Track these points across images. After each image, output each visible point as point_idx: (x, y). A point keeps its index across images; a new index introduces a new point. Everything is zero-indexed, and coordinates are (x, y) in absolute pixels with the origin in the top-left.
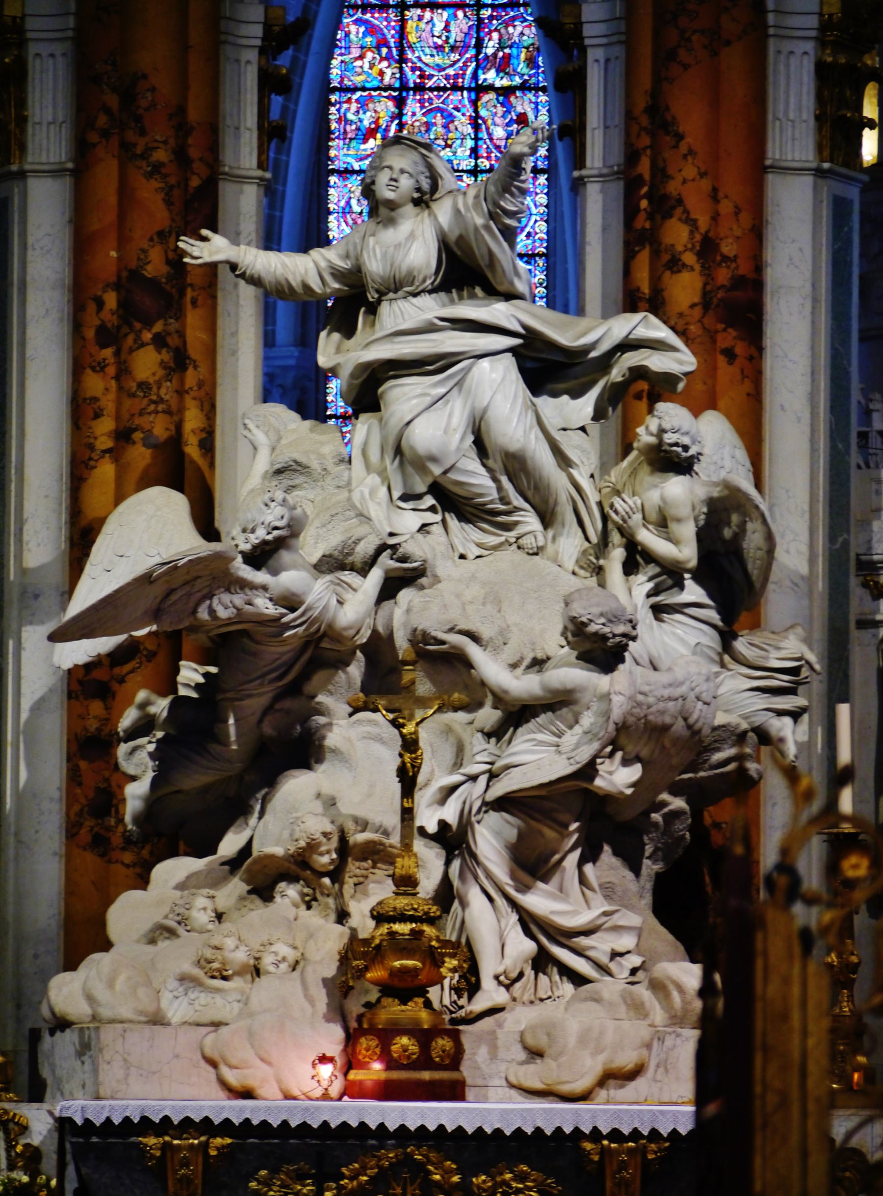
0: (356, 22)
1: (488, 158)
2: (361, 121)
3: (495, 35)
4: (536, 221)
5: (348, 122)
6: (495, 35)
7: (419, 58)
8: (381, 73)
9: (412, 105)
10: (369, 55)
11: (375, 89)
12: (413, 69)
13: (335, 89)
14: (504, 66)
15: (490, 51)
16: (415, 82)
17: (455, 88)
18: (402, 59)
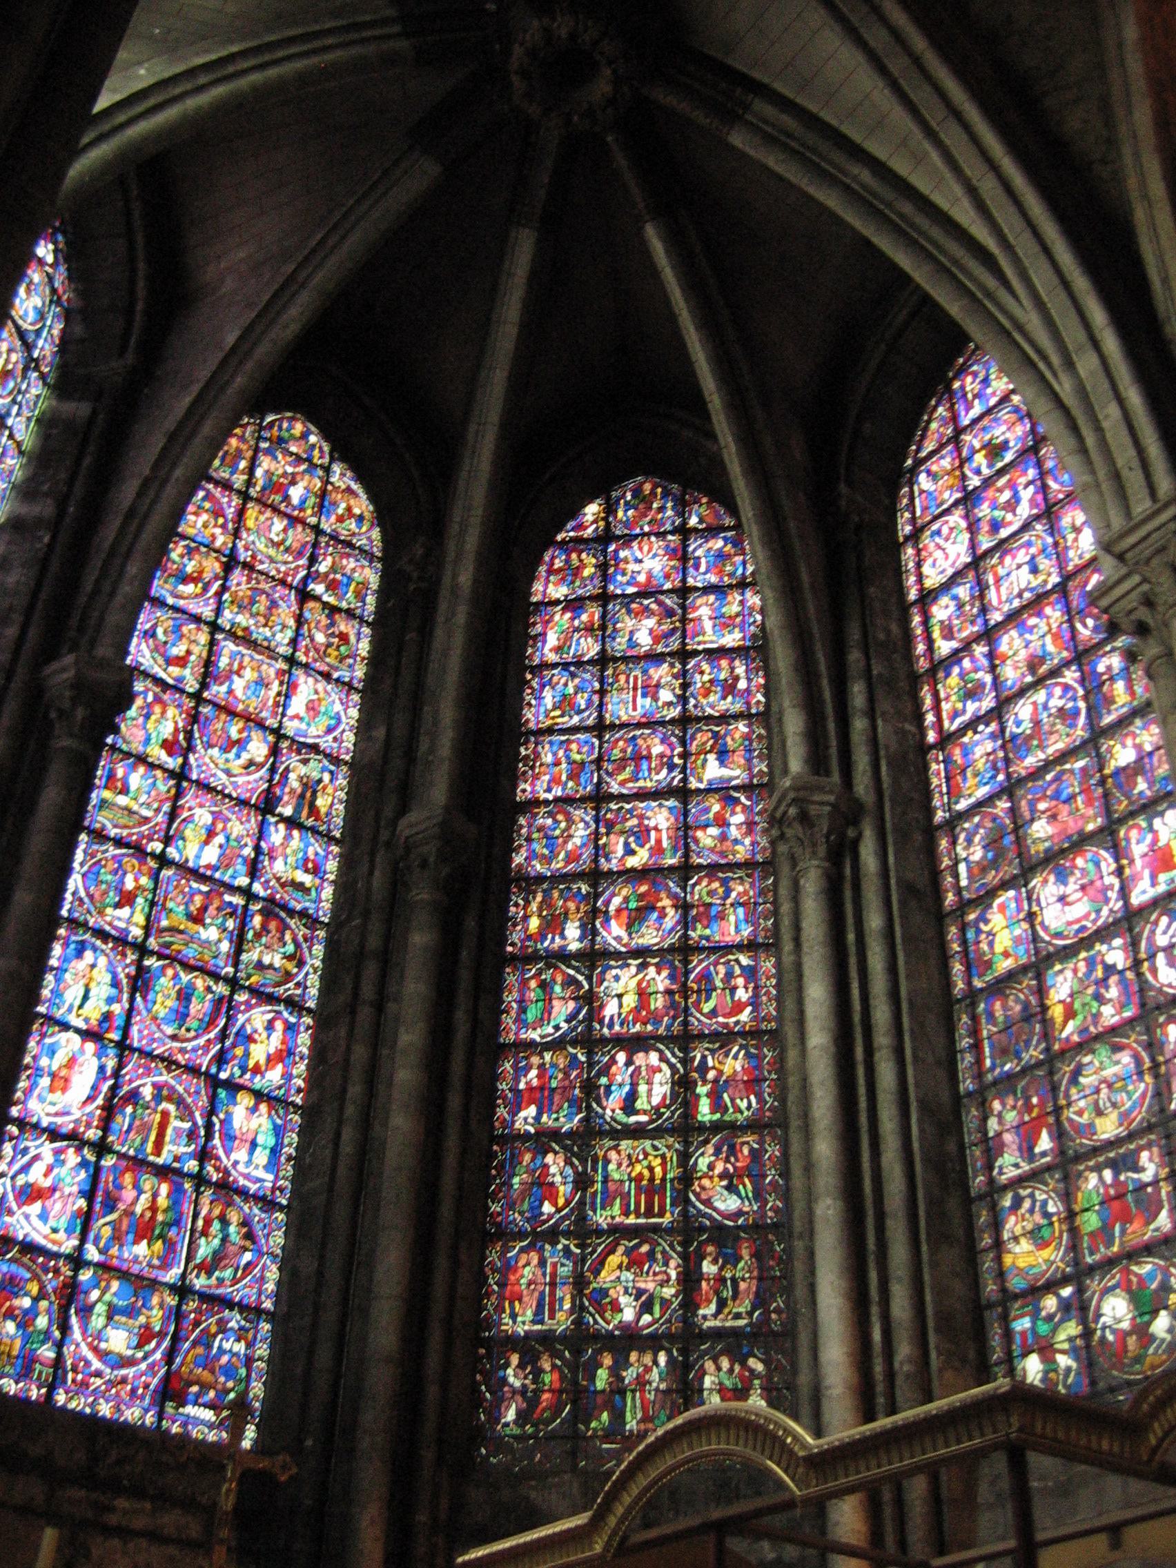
1: (306, 654)
17: (283, 582)
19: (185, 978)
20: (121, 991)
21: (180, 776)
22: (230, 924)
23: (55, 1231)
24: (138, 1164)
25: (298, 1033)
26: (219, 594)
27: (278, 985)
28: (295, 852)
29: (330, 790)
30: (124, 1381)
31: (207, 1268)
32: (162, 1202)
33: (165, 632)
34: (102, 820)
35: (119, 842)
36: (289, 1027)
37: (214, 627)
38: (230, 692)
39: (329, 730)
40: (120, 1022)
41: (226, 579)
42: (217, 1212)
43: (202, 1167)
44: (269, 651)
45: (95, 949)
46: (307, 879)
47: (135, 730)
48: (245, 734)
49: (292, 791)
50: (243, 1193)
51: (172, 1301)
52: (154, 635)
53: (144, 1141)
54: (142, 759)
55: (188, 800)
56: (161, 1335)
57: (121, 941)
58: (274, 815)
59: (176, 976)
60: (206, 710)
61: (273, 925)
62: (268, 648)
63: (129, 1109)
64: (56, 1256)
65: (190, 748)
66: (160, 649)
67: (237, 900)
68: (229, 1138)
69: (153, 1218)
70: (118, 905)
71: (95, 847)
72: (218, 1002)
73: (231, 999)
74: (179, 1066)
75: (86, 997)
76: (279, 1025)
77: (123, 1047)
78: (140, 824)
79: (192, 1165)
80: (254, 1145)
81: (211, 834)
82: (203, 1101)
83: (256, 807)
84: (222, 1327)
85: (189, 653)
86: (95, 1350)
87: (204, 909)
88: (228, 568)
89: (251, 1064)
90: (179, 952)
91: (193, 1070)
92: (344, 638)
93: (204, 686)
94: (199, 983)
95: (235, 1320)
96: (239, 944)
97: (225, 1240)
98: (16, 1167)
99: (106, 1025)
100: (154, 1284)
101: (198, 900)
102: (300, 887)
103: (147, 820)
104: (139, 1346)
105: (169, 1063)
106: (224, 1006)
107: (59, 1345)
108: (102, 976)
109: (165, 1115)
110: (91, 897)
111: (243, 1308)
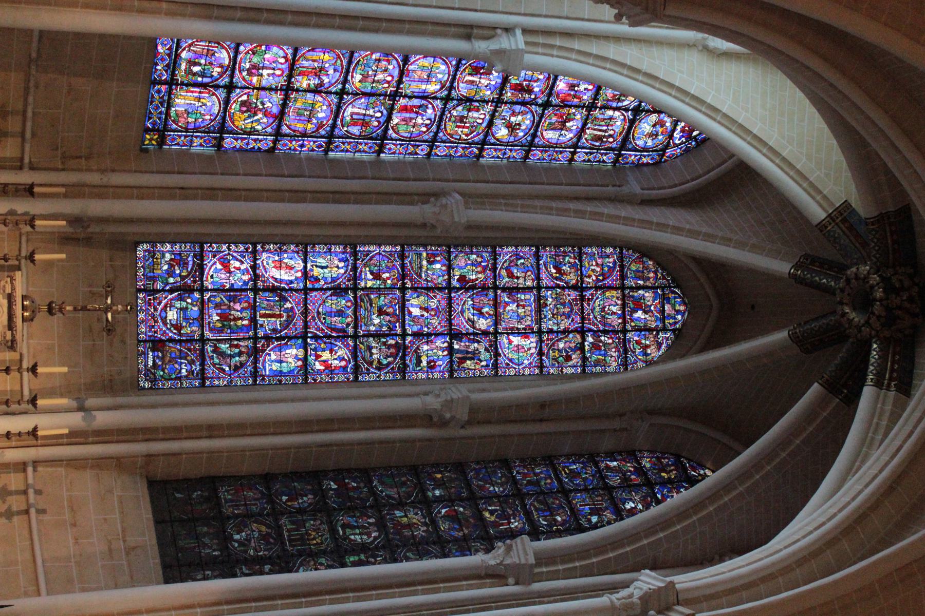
0: (614, 261)
1: (548, 339)
2: (565, 265)
3: (610, 341)
5: (564, 257)
6: (610, 341)
7: (597, 298)
8: (589, 276)
9: (574, 294)
10: (598, 269)
12: (592, 295)
13: (580, 249)
14: (595, 346)
15: (603, 338)
17: (583, 319)
18: (597, 288)
19: (350, 312)
22: (385, 329)
23: (212, 277)
24: (253, 308)
26: (558, 286)
27: (364, 359)
29: (477, 367)
30: (156, 322)
31: (216, 350)
32: (239, 323)
34: (411, 256)
35: (403, 266)
36: (345, 368)
38: (507, 304)
39: (511, 360)
40: (317, 286)
41: (569, 288)
42: (243, 350)
43: (262, 338)
44: (539, 321)
46: (424, 363)
50: (256, 361)
51: (196, 337)
52: (518, 259)
53: (265, 309)
54: (450, 268)
56: (180, 334)
57: (356, 278)
59: (349, 307)
60: (491, 294)
61: (392, 350)
62: (541, 318)
63: (277, 299)
64: (202, 281)
65: (467, 290)
66: (512, 263)
67: (399, 331)
68: (280, 348)
69: (231, 320)
70: (372, 273)
72: (343, 330)
73: (348, 337)
74: (306, 317)
75: (322, 268)
76: (343, 363)
77: (306, 291)
78: (416, 274)
79: (261, 334)
80: (281, 362)
81: (426, 309)
82: (293, 333)
83: (451, 329)
84: (192, 362)
85: (518, 278)
86: (166, 306)
87: (388, 314)
88: (574, 287)
89: (320, 353)
91: (306, 326)
92: (568, 358)
93: (504, 289)
94: (349, 319)
95: (197, 368)
96: (377, 335)
97: (231, 356)
98: (235, 254)
100: (202, 327)
101: (390, 310)
102: (419, 362)
103: (420, 277)
104: (172, 325)
105: (306, 312)
106: (342, 335)
107: (163, 290)
108: (335, 272)
109: (280, 316)
110: (371, 259)
111: (203, 370)
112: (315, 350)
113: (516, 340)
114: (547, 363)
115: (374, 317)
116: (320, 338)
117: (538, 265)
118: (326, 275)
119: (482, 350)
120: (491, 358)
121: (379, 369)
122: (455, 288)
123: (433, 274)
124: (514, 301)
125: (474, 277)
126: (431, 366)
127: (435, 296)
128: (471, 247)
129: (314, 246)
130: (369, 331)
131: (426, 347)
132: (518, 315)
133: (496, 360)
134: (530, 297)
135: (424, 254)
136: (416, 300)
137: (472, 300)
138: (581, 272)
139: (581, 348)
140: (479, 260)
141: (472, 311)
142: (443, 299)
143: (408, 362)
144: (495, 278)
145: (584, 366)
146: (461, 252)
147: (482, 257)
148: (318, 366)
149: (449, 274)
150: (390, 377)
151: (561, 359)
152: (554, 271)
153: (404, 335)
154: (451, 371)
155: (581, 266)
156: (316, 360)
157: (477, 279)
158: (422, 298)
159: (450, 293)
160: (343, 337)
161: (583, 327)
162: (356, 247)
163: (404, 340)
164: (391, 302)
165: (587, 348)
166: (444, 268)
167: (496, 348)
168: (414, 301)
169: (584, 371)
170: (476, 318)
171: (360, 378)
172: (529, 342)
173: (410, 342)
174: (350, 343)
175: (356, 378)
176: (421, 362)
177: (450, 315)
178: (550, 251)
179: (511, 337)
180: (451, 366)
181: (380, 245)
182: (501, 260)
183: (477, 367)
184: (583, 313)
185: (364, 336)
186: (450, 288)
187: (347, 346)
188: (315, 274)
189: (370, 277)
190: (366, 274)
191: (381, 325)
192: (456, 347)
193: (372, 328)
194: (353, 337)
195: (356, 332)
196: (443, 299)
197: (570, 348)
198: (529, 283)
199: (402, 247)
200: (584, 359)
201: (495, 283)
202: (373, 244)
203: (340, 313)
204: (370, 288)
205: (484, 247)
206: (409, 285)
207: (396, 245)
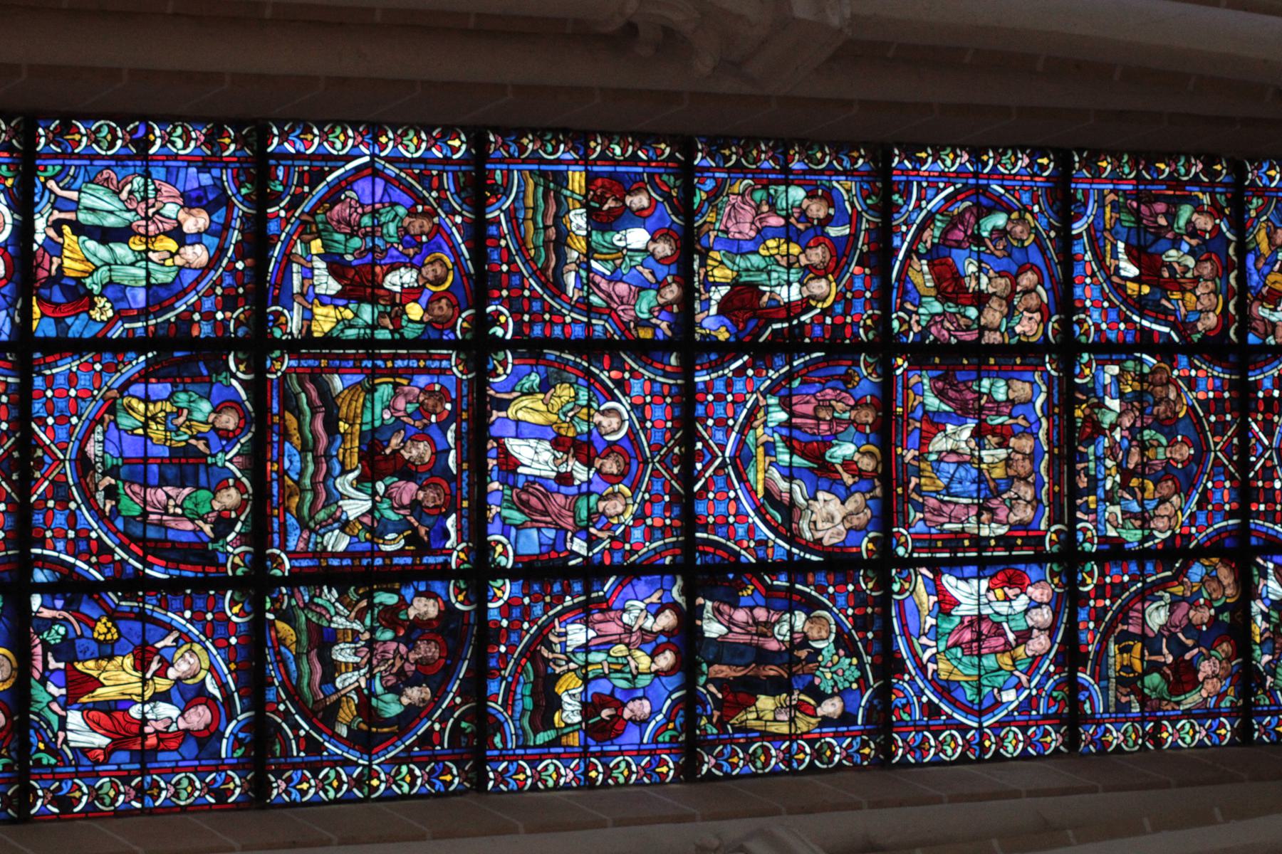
1: (1100, 590)
2: (1175, 244)
4: (963, 729)
5: (1174, 204)
11: (1242, 279)
13: (1238, 170)
16: (1258, 385)
17: (1245, 493)
19: (229, 460)
20: (144, 313)
21: (686, 345)
22: (393, 543)
25: (201, 772)
26: (1147, 341)
27: (294, 693)
28: (621, 667)
29: (803, 724)
33: (1000, 233)
34: (519, 188)
35: (478, 232)
36: (207, 739)
37: (1066, 348)
38: (934, 423)
39: (945, 689)
40: (77, 327)
41: (1189, 349)
45: (221, 232)
46: (571, 712)
47: (747, 214)
48: (848, 479)
49: (766, 629)
52: (983, 211)
54: (688, 246)
55: (642, 380)
58: (688, 592)
59: (228, 437)
60: (866, 376)
61: (427, 650)
62: (1075, 492)
65: (762, 355)
66: (960, 229)
67: (456, 550)
70: (337, 267)
71: (448, 182)
72: (198, 552)
73: (223, 583)
74: (25, 486)
75: (105, 235)
76: (199, 717)
78: (539, 274)
81: (583, 448)
83: (690, 545)
85: (981, 300)
87: (407, 471)
88: (1212, 348)
89: (89, 667)
90: (285, 435)
92: (1183, 677)
93: (921, 354)
94: (230, 498)
96: (357, 576)
99: (58, 296)
101: (420, 451)
102: (547, 703)
103: (558, 288)
106: (195, 574)
110: (333, 196)
112: (66, 650)
113: (967, 593)
114: (1096, 701)
115: (344, 484)
116: (92, 589)
117: (1066, 240)
118: (121, 274)
119: (826, 646)
120: (862, 681)
121: (364, 741)
122: (710, 344)
123: (614, 279)
124: (961, 415)
125: (795, 293)
126: (603, 721)
127: (620, 384)
128: (782, 149)
129: (67, 128)
130: (324, 553)
131: (577, 634)
132: (980, 479)
133: (885, 692)
134: (1030, 391)
135: (577, 179)
136: (536, 402)
137: (786, 405)
138: (1242, 279)
139: (1234, 628)
140: (818, 210)
141: (784, 457)
142: (658, 396)
143: (495, 706)
144: (883, 300)
145: (1245, 713)
146: (738, 169)
147: (830, 197)
148: (81, 733)
149: (685, 277)
150: (411, 780)
151: (1154, 679)
152: (1130, 270)
153: (480, 572)
154: (690, 749)
155: (1242, 250)
156: (68, 702)
157: (805, 305)
158: (565, 392)
159: (687, 371)
160: (200, 585)
161: (1244, 531)
162: (265, 138)
163: (480, 596)
164: (422, 412)
165: (1259, 625)
166: (663, 249)
167: (886, 636)
168: (529, 410)
169: (1243, 733)
170: (799, 491)
171: (278, 788)
172: (1021, 603)
173: (506, 610)
174: (233, 614)
175: (259, 788)
176: (557, 704)
177: (688, 477)
178: (1116, 178)
179: (949, 581)
180: (690, 724)
181: (374, 131)
182: (910, 211)
183: (803, 724)
184: (1244, 466)
185: (296, 579)
186: (686, 345)
187: (216, 630)
188: (72, 266)
189: (328, 285)
190: (309, 273)
191: (375, 527)
192: (713, 629)
193: (337, 541)
194: (244, 585)
195: (259, 560)
196: (658, 396)
197: (1190, 628)
198: (1027, 326)
199: (478, 141)
200: (1247, 679)
201: (883, 322)
202: (343, 123)
203: (186, 466)
204: (329, 340)
205: (839, 148)
206: (504, 330)
207: (449, 132)
